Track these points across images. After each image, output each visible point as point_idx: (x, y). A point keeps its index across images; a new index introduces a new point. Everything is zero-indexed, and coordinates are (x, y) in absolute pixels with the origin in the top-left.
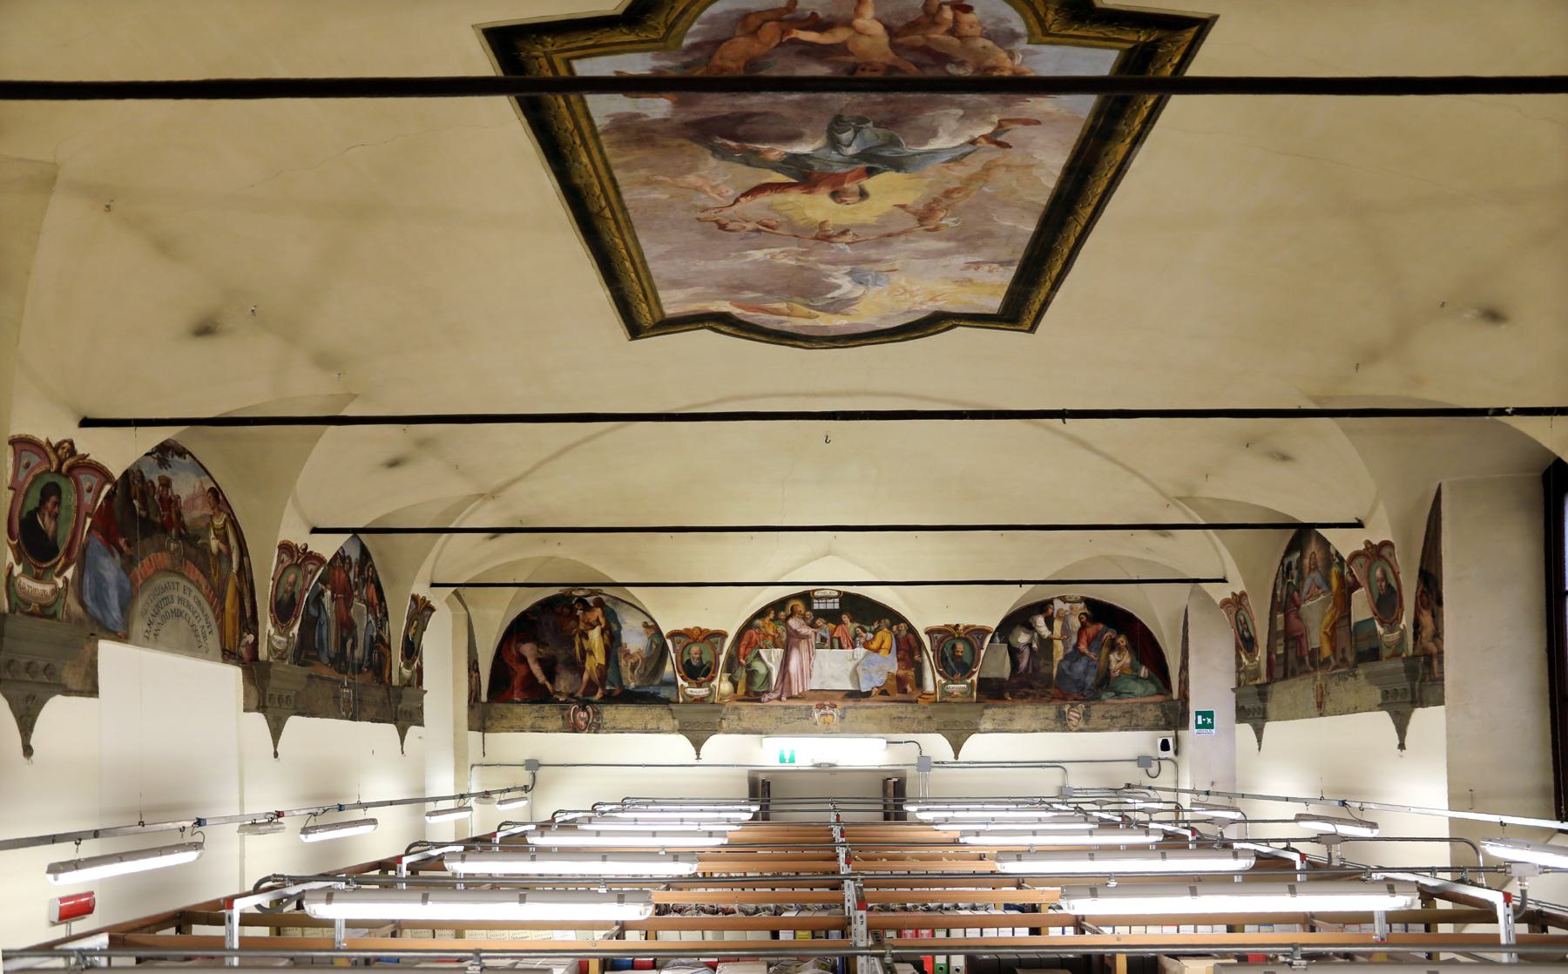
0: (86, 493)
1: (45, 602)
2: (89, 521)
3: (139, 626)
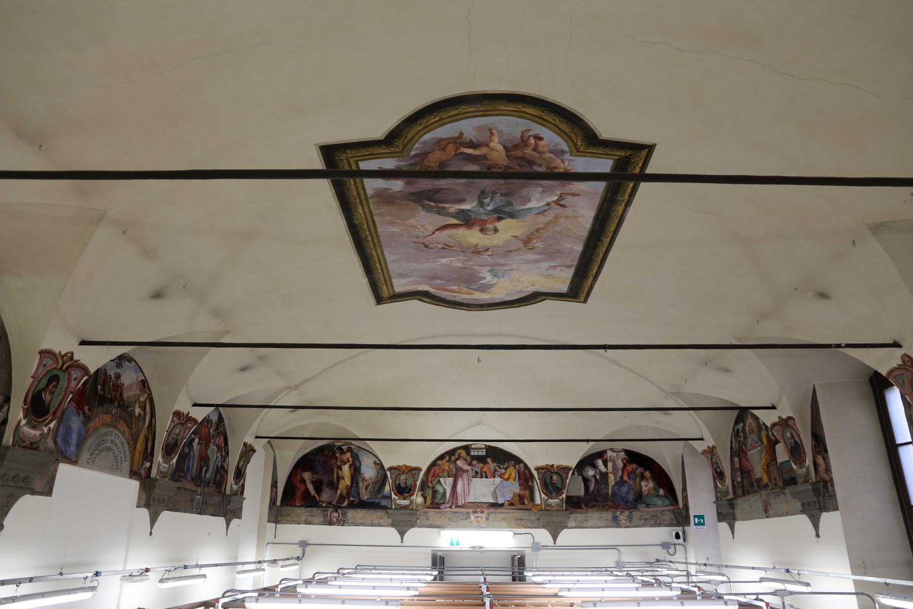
1: (33, 441)
2: (71, 396)
3: (85, 456)
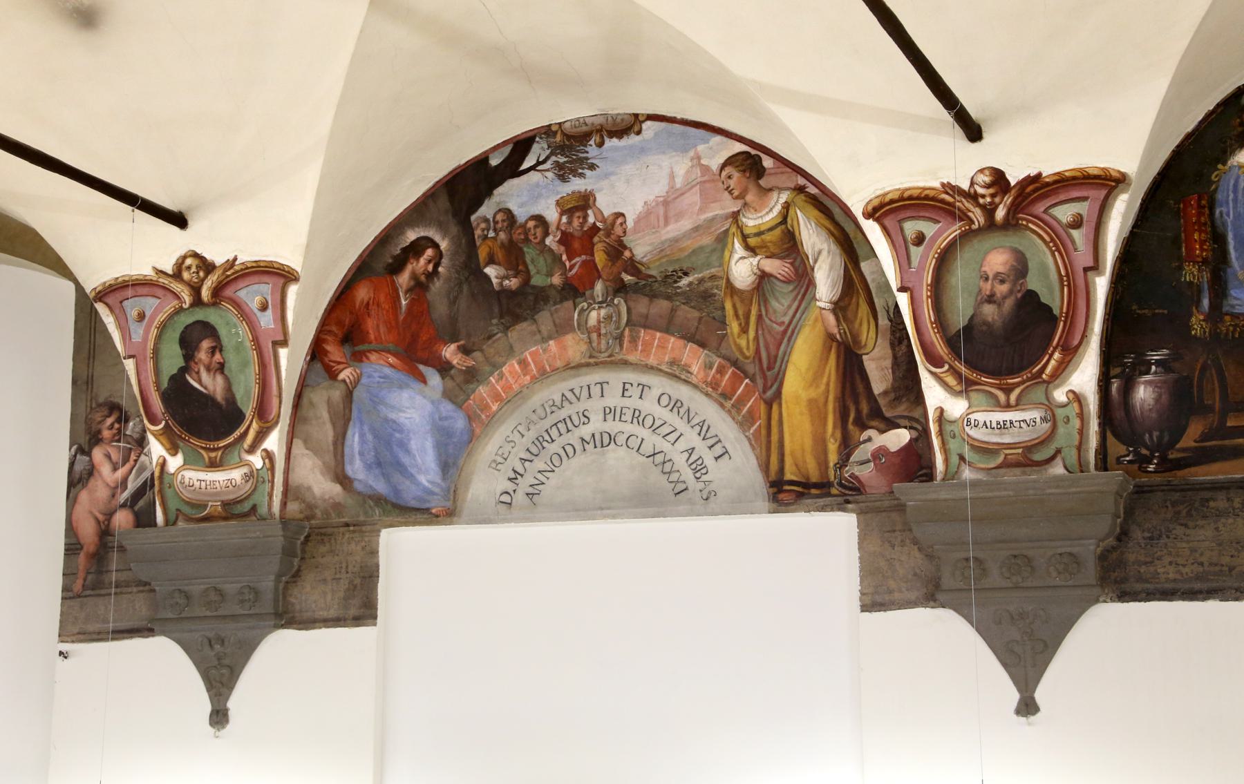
0: (259, 314)
1: (232, 497)
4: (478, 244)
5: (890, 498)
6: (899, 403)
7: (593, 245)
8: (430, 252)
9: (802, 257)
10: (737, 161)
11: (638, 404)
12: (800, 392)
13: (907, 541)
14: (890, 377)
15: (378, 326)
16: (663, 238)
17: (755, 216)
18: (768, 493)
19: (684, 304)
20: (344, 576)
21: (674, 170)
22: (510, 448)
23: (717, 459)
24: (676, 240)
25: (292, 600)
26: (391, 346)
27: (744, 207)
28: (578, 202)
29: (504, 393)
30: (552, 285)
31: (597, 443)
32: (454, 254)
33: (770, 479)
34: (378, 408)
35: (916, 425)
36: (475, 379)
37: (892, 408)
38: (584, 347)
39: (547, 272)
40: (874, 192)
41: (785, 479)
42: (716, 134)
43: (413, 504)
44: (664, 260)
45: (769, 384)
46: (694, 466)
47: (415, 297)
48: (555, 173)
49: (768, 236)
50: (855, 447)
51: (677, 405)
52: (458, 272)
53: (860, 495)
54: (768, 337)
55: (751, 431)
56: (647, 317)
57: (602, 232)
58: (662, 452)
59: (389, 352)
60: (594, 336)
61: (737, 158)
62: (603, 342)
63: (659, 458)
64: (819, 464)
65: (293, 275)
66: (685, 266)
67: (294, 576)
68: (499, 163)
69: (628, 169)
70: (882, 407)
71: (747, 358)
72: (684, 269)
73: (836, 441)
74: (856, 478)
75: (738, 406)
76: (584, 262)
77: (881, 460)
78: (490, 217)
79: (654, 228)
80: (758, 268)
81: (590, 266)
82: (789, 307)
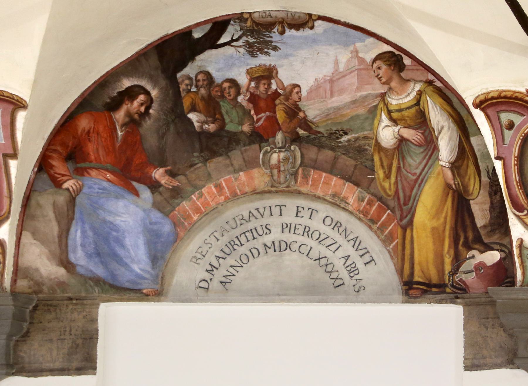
4: (183, 95)
5: (485, 296)
6: (494, 234)
7: (275, 106)
8: (142, 97)
9: (430, 130)
10: (385, 57)
11: (308, 222)
12: (426, 222)
13: (497, 325)
14: (488, 216)
15: (97, 149)
16: (329, 106)
17: (397, 98)
18: (402, 289)
19: (344, 154)
20: (67, 337)
21: (338, 58)
22: (208, 249)
23: (366, 264)
24: (339, 109)
25: (22, 354)
26: (109, 166)
27: (389, 90)
28: (264, 73)
29: (203, 207)
30: (242, 132)
31: (276, 248)
32: (162, 101)
33: (404, 280)
34: (98, 212)
35: (504, 249)
36: (179, 196)
37: (489, 237)
38: (267, 179)
39: (239, 121)
40: (481, 91)
41: (414, 280)
42: (370, 37)
43: (127, 285)
44: (330, 122)
45: (405, 214)
46: (349, 268)
47: (130, 130)
48: (246, 50)
49: (406, 112)
50: (462, 262)
51: (337, 225)
52: (165, 114)
53: (466, 293)
54: (404, 182)
55: (391, 247)
56: (316, 161)
57: (282, 97)
58: (326, 257)
59: (107, 170)
60: (275, 171)
61: (385, 55)
62: (282, 176)
63: (323, 262)
64: (438, 272)
65: (22, 103)
66: (345, 128)
67: (23, 336)
68: (200, 36)
69: (304, 53)
70: (482, 235)
71: (389, 196)
72: (345, 130)
73: (450, 257)
74: (463, 282)
75: (382, 228)
76: (268, 118)
77: (480, 271)
78: (193, 76)
79: (322, 98)
80: (398, 134)
81: (273, 121)
82: (420, 163)
